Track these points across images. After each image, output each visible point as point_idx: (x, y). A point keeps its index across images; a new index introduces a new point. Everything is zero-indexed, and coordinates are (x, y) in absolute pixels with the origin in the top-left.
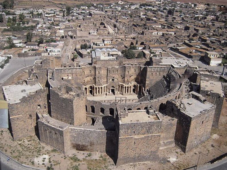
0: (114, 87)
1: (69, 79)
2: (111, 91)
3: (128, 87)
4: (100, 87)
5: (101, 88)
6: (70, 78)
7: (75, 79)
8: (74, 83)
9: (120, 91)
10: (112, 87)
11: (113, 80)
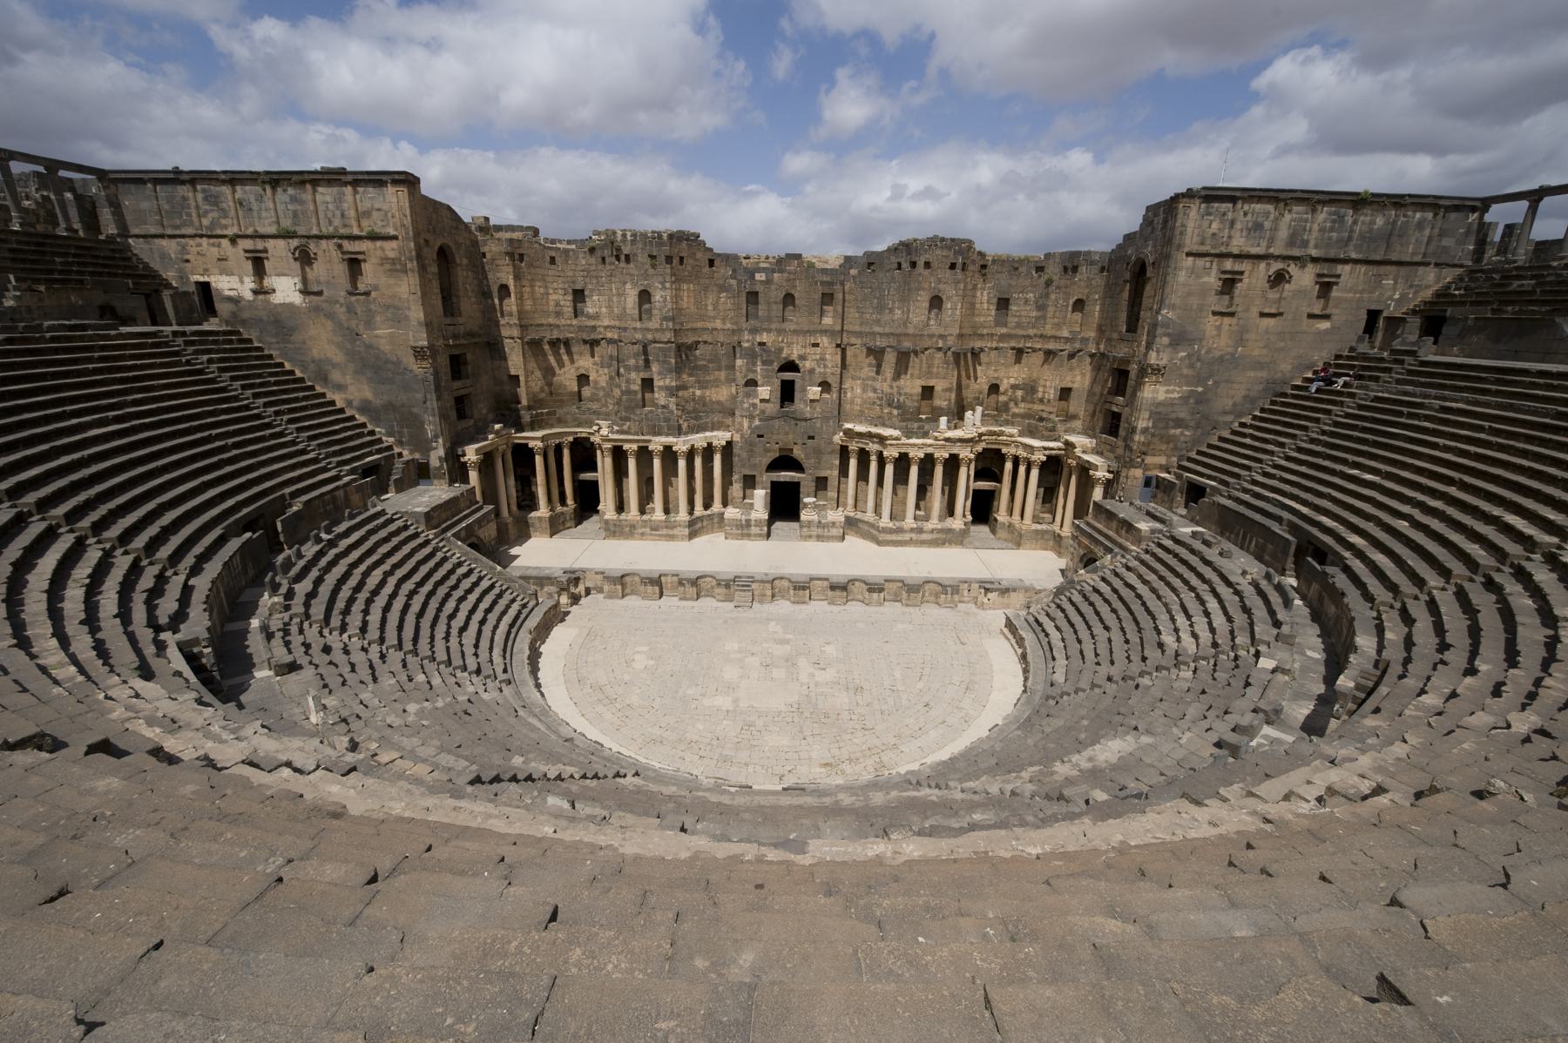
0: (796, 466)
1: (277, 298)
2: (760, 495)
3: (927, 463)
4: (657, 443)
5: (669, 455)
6: (286, 289)
7: (340, 311)
8: (336, 355)
9: (850, 501)
10: (775, 466)
11: (787, 392)
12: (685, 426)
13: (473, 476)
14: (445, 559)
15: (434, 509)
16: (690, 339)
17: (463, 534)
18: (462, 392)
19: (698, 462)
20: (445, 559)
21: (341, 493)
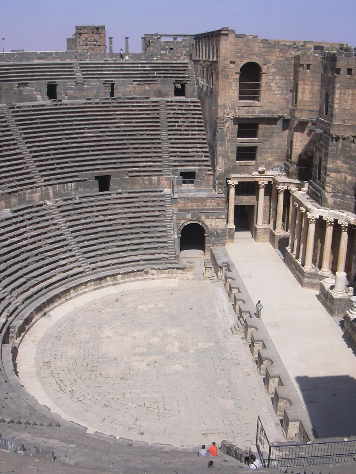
12: (330, 201)
13: (232, 192)
14: (163, 221)
15: (181, 198)
16: (348, 134)
17: (189, 216)
18: (247, 145)
19: (329, 231)
20: (163, 221)
21: (156, 178)
